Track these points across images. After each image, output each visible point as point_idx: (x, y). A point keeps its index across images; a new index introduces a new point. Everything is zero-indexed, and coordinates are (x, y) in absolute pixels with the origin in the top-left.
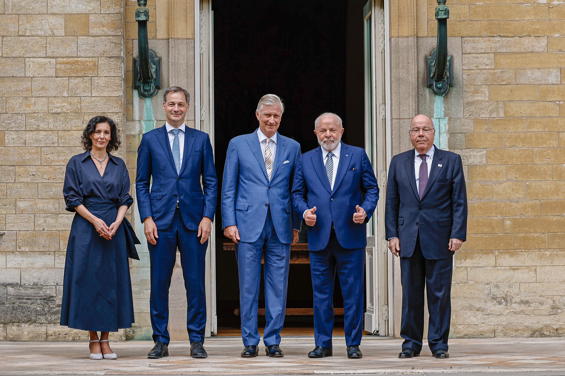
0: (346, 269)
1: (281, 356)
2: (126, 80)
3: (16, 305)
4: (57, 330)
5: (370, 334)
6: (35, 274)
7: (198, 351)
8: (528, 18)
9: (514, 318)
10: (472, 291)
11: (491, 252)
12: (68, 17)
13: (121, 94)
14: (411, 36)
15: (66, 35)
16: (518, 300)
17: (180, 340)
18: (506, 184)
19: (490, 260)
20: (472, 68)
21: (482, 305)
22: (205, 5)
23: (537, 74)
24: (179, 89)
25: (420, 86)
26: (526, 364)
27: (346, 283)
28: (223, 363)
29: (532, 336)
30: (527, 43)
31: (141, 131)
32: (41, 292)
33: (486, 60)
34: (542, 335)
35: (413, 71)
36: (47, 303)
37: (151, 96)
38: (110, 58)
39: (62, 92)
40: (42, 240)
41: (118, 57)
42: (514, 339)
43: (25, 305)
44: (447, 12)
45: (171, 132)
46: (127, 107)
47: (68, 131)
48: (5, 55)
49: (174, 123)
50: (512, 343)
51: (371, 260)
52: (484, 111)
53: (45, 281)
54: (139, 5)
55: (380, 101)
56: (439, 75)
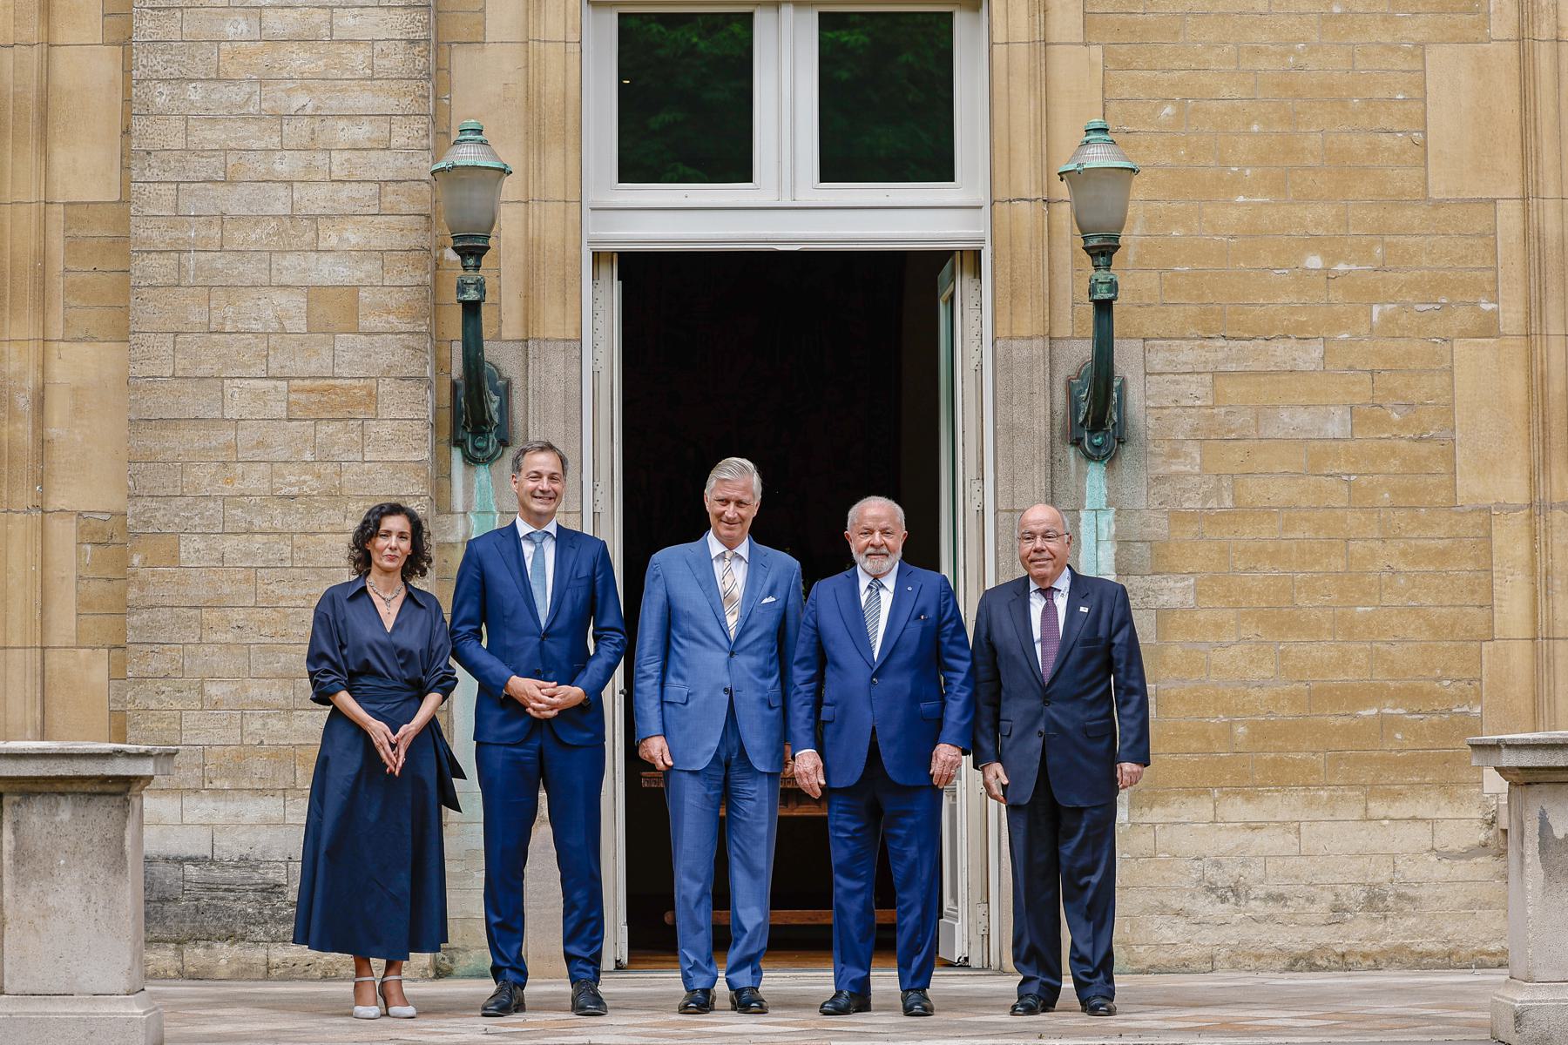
0: (902, 827)
1: (762, 1010)
2: (436, 427)
3: (202, 903)
4: (289, 955)
5: (950, 965)
6: (243, 838)
7: (588, 1002)
8: (1284, 299)
9: (1253, 931)
10: (1166, 874)
11: (1206, 791)
12: (315, 293)
13: (427, 455)
14: (1038, 337)
15: (309, 332)
16: (1262, 894)
17: (548, 976)
18: (1238, 648)
19: (1204, 808)
20: (1166, 404)
21: (1186, 903)
22: (604, 269)
23: (1303, 417)
24: (548, 447)
25: (1057, 441)
26: (1278, 1028)
27: (902, 857)
28: (641, 1026)
29: (1291, 968)
30: (1282, 352)
31: (467, 534)
32: (256, 876)
33: (1195, 388)
34: (1313, 967)
35: (1041, 409)
36: (269, 899)
37: (489, 460)
38: (403, 379)
39: (299, 452)
40: (258, 766)
41: (419, 379)
42: (1253, 974)
43: (221, 903)
44: (1113, 286)
45: (528, 537)
46: (438, 484)
47: (314, 533)
48: (181, 374)
49: (538, 519)
50: (1249, 983)
51: (953, 808)
52: (1191, 495)
53: (263, 853)
54: (465, 268)
55: (972, 472)
56: (1096, 419)
